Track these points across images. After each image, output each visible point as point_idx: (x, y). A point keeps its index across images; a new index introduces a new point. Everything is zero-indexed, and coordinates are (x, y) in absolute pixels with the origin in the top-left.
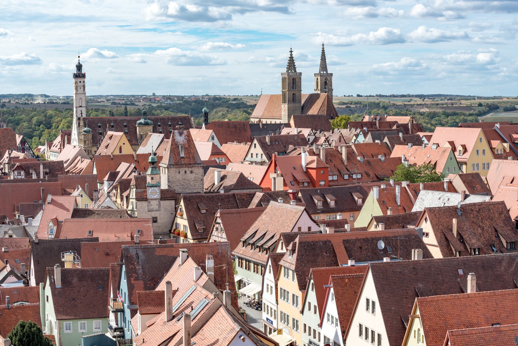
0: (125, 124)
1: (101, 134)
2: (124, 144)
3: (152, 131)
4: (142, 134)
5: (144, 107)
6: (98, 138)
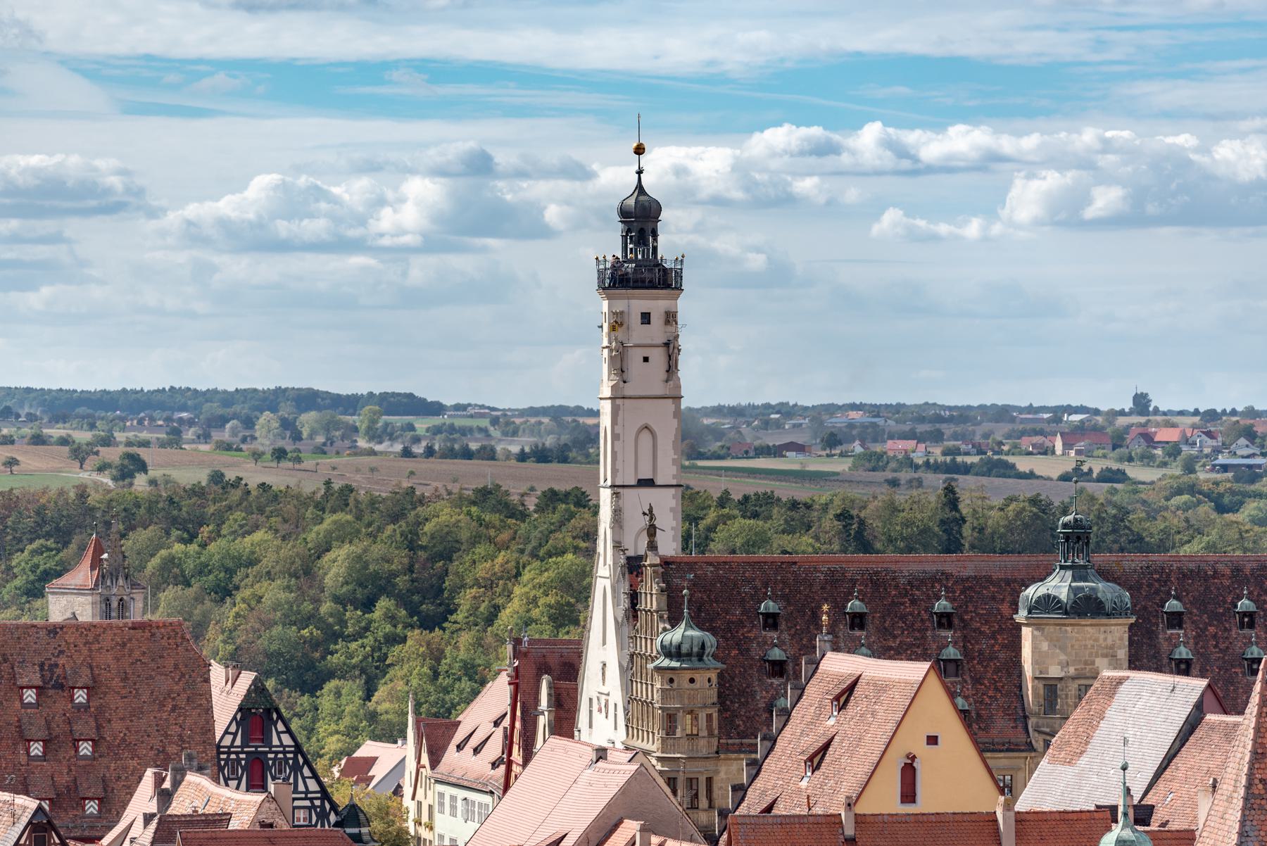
0: (942, 605)
1: (778, 668)
2: (933, 740)
3: (1123, 654)
4: (1054, 672)
5: (1070, 487)
6: (761, 698)
